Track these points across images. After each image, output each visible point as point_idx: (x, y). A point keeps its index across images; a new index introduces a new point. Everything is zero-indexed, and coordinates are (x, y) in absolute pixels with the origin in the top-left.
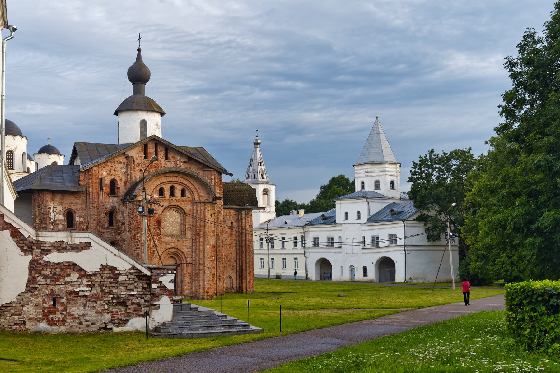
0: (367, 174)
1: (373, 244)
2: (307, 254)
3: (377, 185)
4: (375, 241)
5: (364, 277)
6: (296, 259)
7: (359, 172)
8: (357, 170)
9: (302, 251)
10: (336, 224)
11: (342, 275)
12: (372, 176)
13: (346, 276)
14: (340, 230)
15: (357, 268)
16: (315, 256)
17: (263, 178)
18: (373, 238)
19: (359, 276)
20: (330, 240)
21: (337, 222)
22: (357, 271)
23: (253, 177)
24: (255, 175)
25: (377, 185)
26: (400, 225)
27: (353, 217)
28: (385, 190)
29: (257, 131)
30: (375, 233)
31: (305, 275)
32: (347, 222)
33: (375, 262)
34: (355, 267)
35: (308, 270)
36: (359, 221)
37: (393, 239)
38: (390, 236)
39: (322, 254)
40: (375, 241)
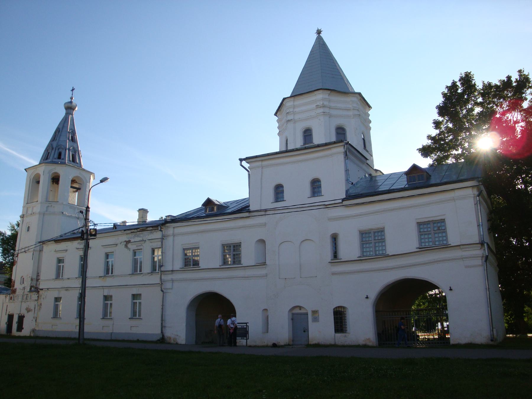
0: (321, 110)
7: (297, 110)
8: (294, 107)
10: (249, 212)
12: (330, 116)
13: (281, 332)
18: (364, 234)
19: (322, 331)
21: (252, 208)
22: (316, 319)
23: (56, 156)
24: (60, 155)
29: (73, 90)
31: (160, 332)
33: (373, 294)
34: (309, 308)
37: (432, 234)
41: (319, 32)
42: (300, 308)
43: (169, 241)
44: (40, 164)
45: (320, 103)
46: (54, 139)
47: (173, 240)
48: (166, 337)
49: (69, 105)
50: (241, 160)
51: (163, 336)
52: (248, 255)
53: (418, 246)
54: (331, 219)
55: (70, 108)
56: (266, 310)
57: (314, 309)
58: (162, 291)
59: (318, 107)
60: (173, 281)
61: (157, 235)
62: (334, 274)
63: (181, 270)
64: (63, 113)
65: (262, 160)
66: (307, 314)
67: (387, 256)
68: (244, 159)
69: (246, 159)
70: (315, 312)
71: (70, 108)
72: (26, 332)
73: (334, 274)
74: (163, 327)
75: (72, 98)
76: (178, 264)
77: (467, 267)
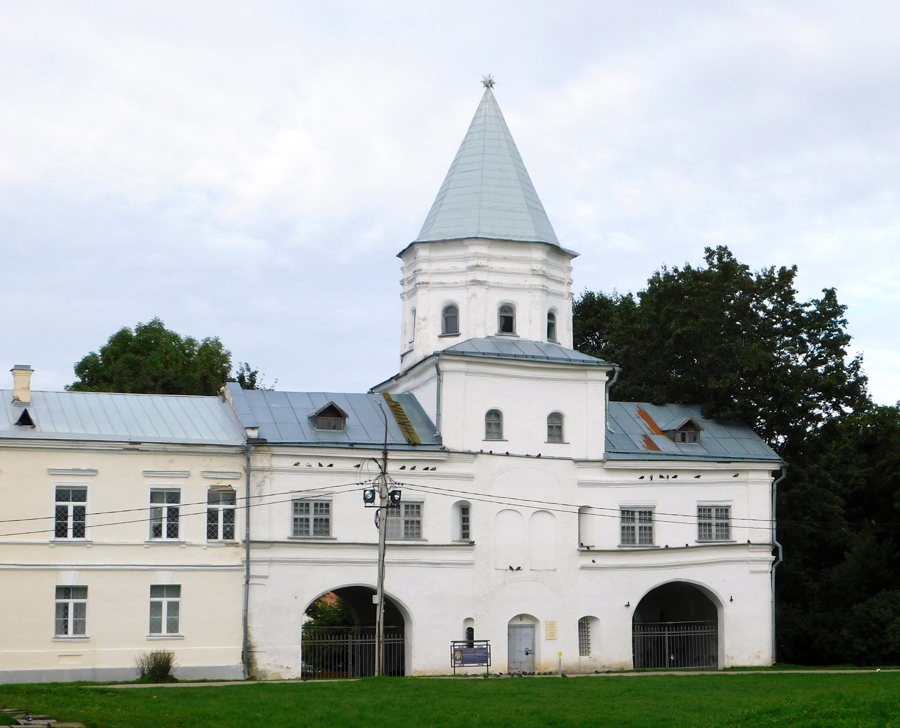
0: (538, 282)
1: (627, 534)
2: (255, 570)
4: (637, 526)
7: (495, 265)
14: (469, 477)
15: (551, 625)
16: (302, 581)
19: (556, 652)
22: (552, 637)
27: (525, 430)
30: (638, 495)
35: (256, 637)
36: (556, 449)
37: (714, 524)
38: (703, 511)
39: (355, 569)
40: (637, 526)
42: (521, 617)
45: (537, 266)
52: (438, 524)
54: (582, 484)
59: (534, 273)
65: (467, 362)
67: (658, 549)
76: (283, 529)
77: (752, 572)
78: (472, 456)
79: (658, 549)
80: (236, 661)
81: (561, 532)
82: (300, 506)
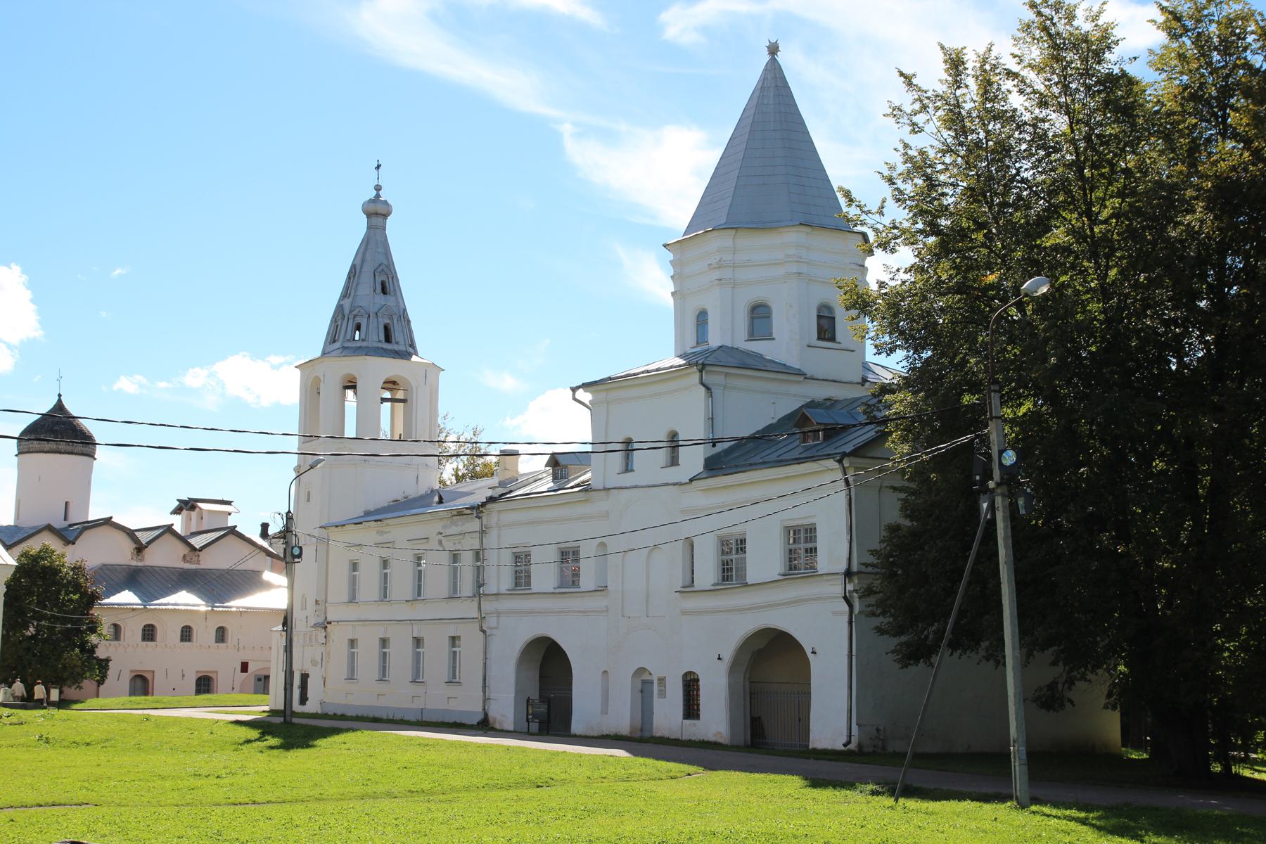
0: (716, 275)
2: (491, 621)
3: (759, 315)
4: (732, 556)
5: (687, 722)
6: (454, 640)
9: (470, 610)
11: (605, 710)
15: (662, 680)
16: (516, 630)
17: (388, 339)
20: (569, 556)
22: (663, 694)
25: (759, 315)
26: (827, 478)
28: (788, 341)
29: (378, 167)
30: (728, 523)
32: (628, 479)
33: (728, 655)
37: (801, 547)
40: (732, 556)
41: (773, 50)
43: (491, 540)
44: (324, 353)
46: (345, 294)
47: (499, 536)
48: (491, 720)
49: (372, 208)
50: (574, 390)
51: (486, 715)
53: (782, 571)
55: (377, 212)
56: (605, 672)
57: (661, 675)
58: (484, 631)
60: (498, 614)
61: (474, 525)
62: (684, 613)
63: (510, 594)
64: (360, 225)
66: (652, 682)
68: (579, 387)
69: (585, 386)
70: (662, 680)
71: (377, 212)
72: (312, 706)
73: (684, 613)
74: (486, 700)
75: (378, 188)
76: (506, 582)
78: (603, 493)
79: (747, 585)
80: (478, 708)
81: (668, 569)
82: (517, 557)
